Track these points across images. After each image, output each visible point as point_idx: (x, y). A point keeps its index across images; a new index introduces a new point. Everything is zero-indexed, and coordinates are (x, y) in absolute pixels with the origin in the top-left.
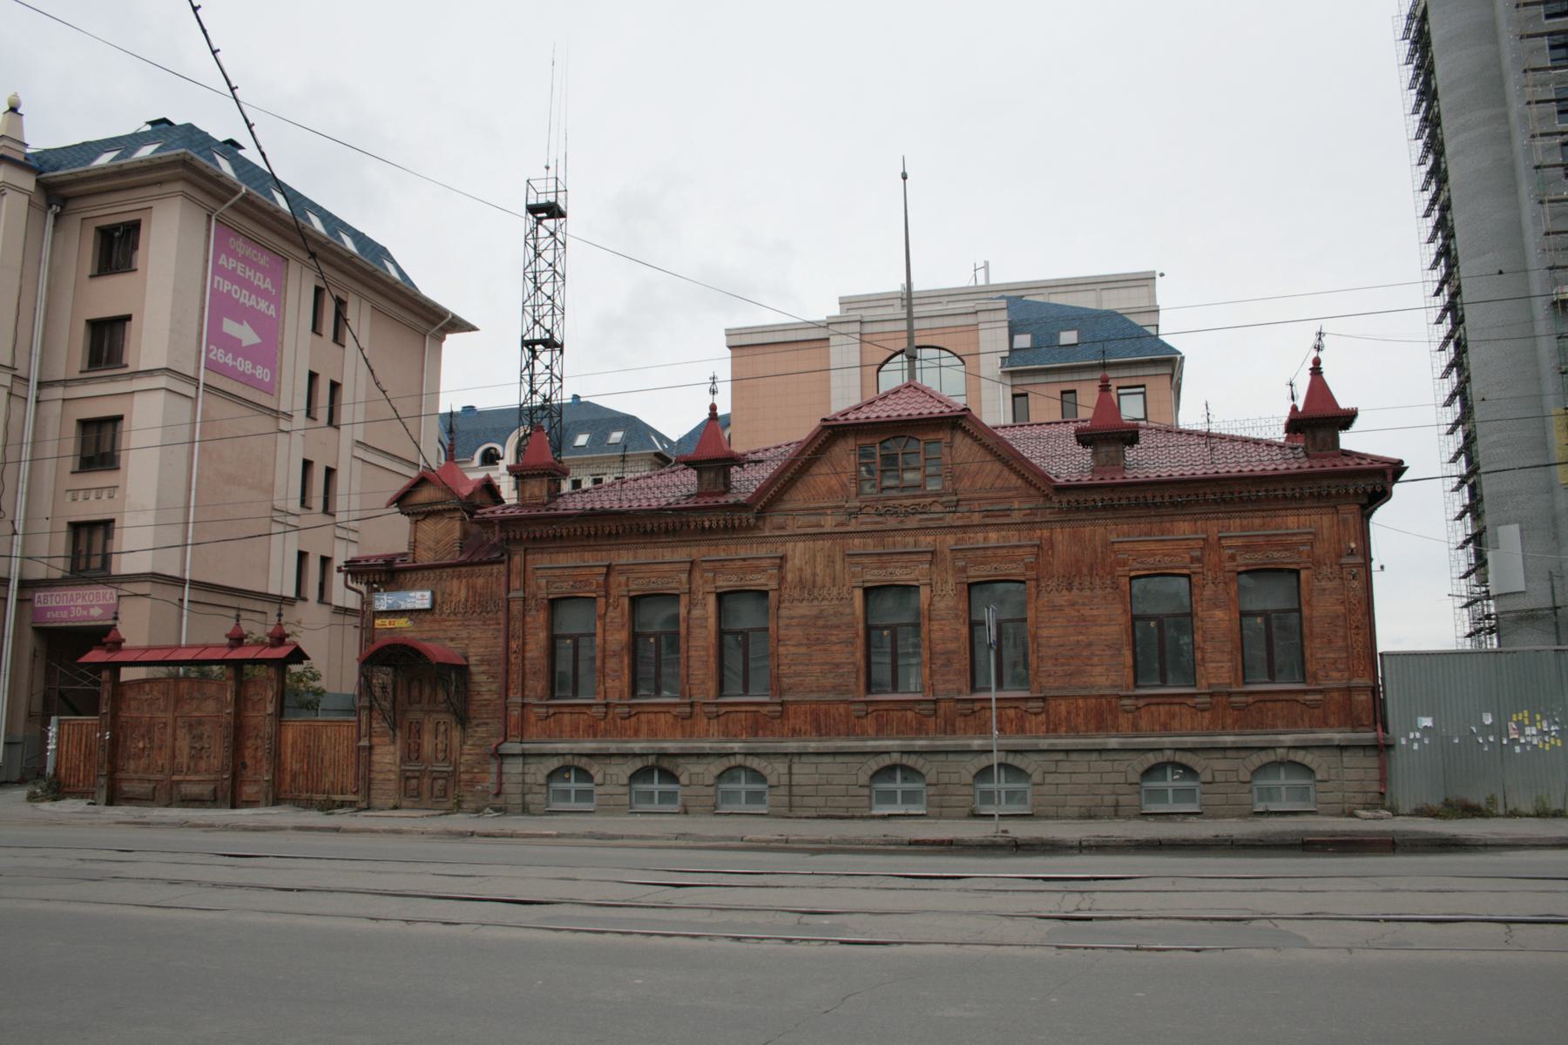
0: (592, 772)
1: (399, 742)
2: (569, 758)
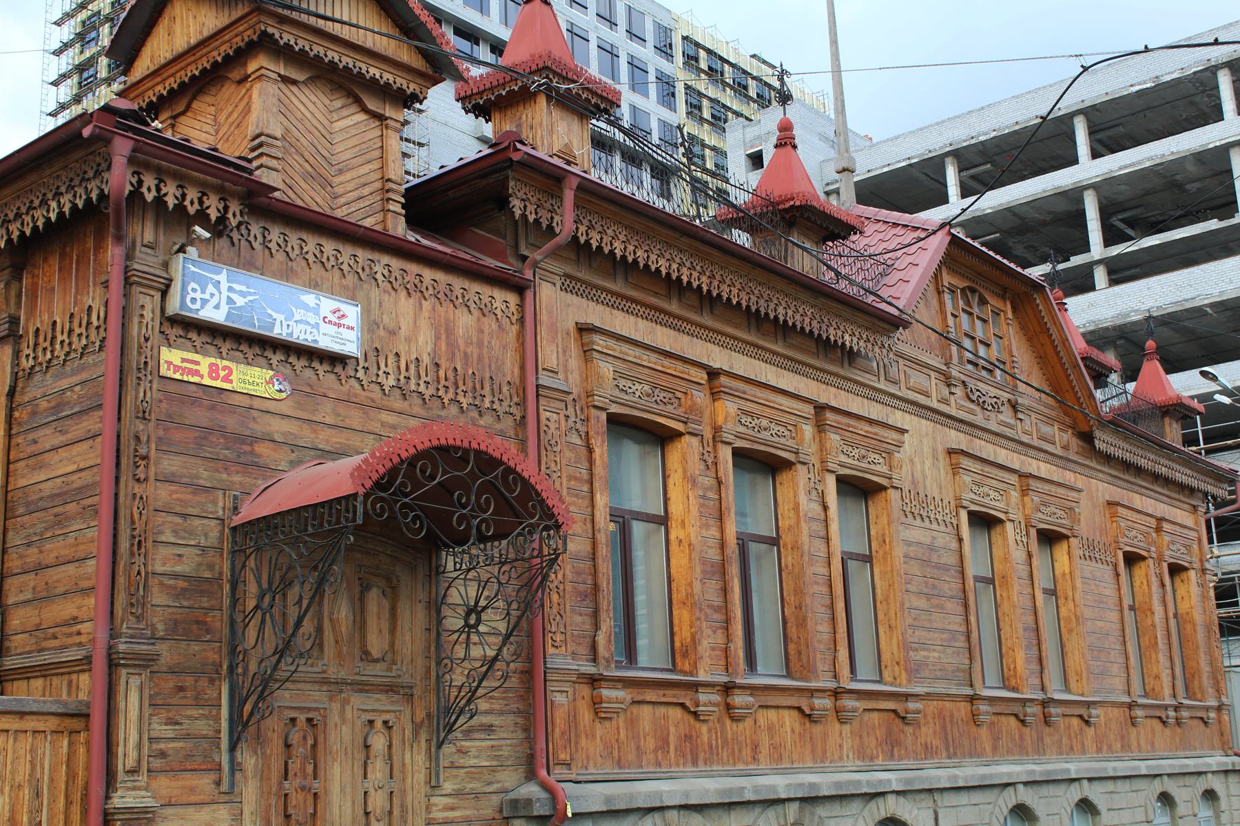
1: (250, 792)
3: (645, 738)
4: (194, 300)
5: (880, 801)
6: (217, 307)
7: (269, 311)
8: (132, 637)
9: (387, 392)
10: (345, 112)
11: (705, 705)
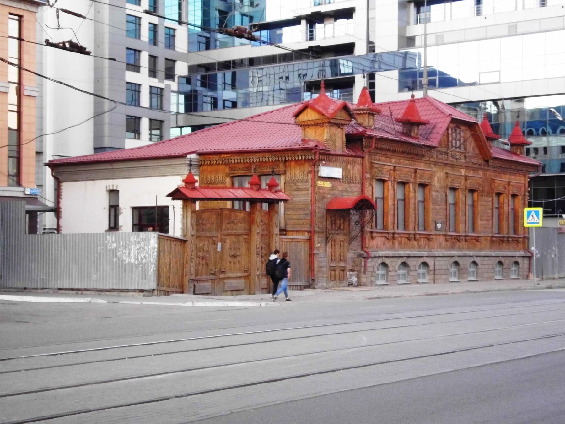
5: (422, 258)
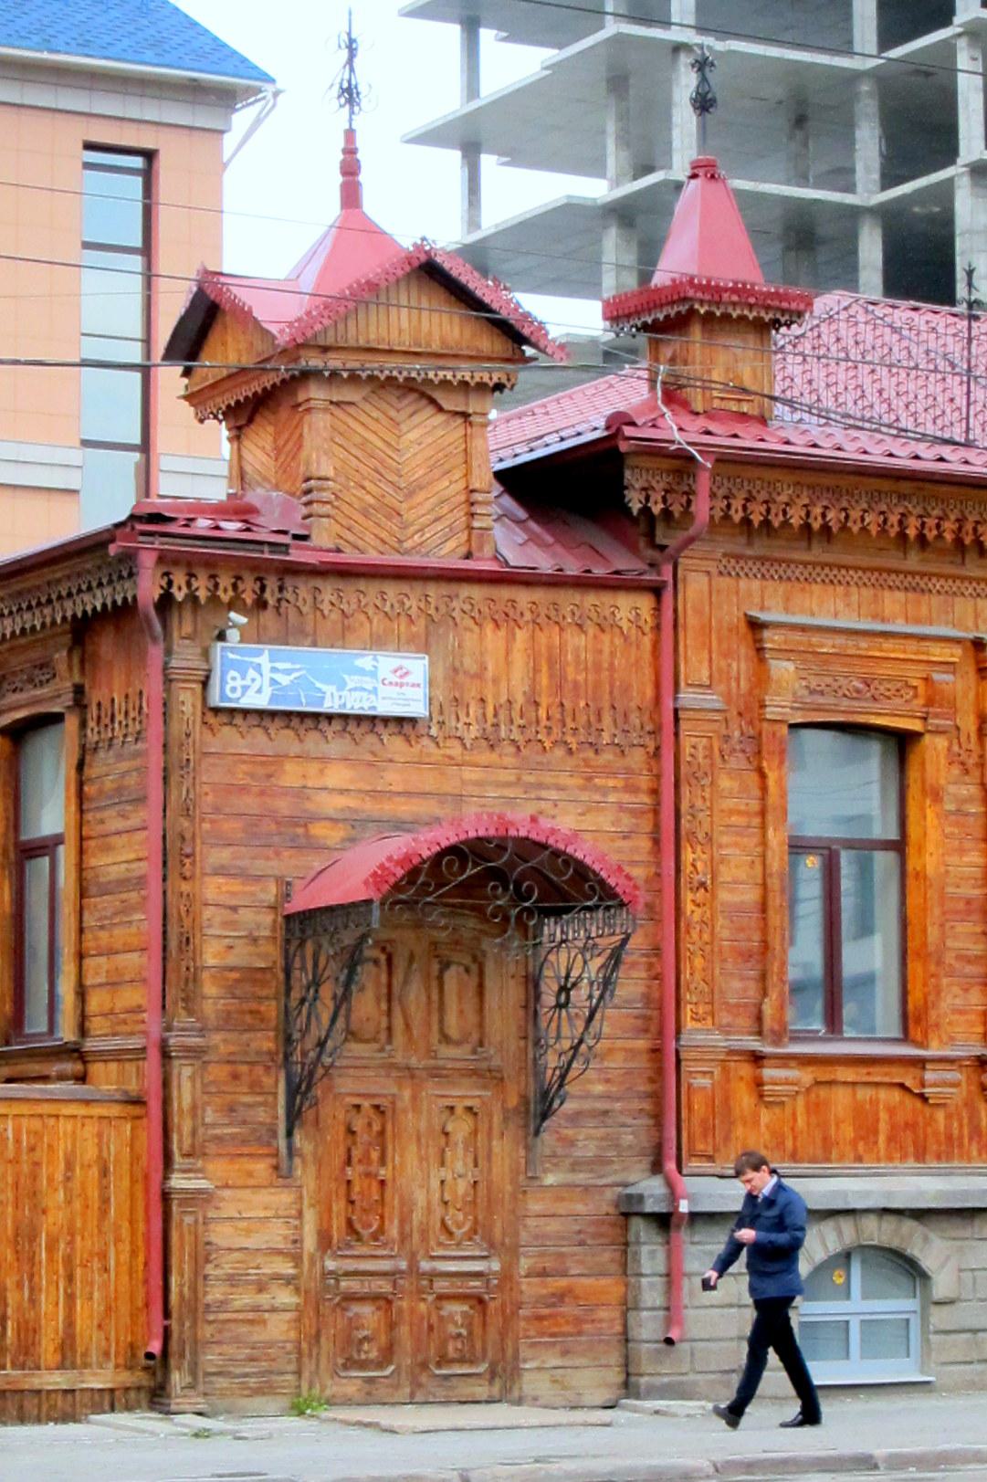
0: (927, 1263)
2: (870, 1223)
3: (837, 1126)
4: (234, 689)
6: (259, 691)
7: (318, 685)
8: (183, 1030)
9: (468, 746)
10: (417, 419)
11: (931, 1086)
